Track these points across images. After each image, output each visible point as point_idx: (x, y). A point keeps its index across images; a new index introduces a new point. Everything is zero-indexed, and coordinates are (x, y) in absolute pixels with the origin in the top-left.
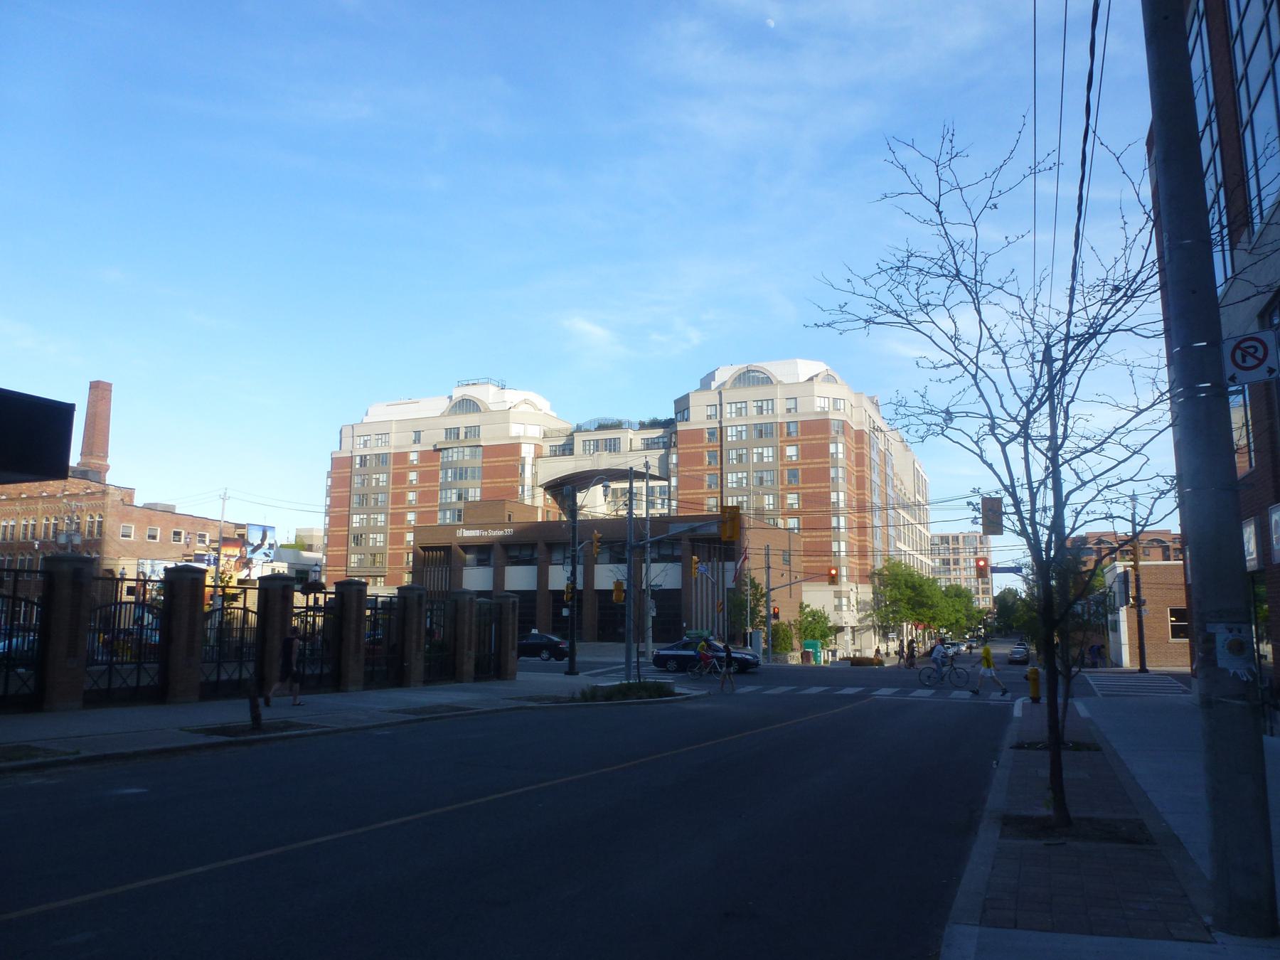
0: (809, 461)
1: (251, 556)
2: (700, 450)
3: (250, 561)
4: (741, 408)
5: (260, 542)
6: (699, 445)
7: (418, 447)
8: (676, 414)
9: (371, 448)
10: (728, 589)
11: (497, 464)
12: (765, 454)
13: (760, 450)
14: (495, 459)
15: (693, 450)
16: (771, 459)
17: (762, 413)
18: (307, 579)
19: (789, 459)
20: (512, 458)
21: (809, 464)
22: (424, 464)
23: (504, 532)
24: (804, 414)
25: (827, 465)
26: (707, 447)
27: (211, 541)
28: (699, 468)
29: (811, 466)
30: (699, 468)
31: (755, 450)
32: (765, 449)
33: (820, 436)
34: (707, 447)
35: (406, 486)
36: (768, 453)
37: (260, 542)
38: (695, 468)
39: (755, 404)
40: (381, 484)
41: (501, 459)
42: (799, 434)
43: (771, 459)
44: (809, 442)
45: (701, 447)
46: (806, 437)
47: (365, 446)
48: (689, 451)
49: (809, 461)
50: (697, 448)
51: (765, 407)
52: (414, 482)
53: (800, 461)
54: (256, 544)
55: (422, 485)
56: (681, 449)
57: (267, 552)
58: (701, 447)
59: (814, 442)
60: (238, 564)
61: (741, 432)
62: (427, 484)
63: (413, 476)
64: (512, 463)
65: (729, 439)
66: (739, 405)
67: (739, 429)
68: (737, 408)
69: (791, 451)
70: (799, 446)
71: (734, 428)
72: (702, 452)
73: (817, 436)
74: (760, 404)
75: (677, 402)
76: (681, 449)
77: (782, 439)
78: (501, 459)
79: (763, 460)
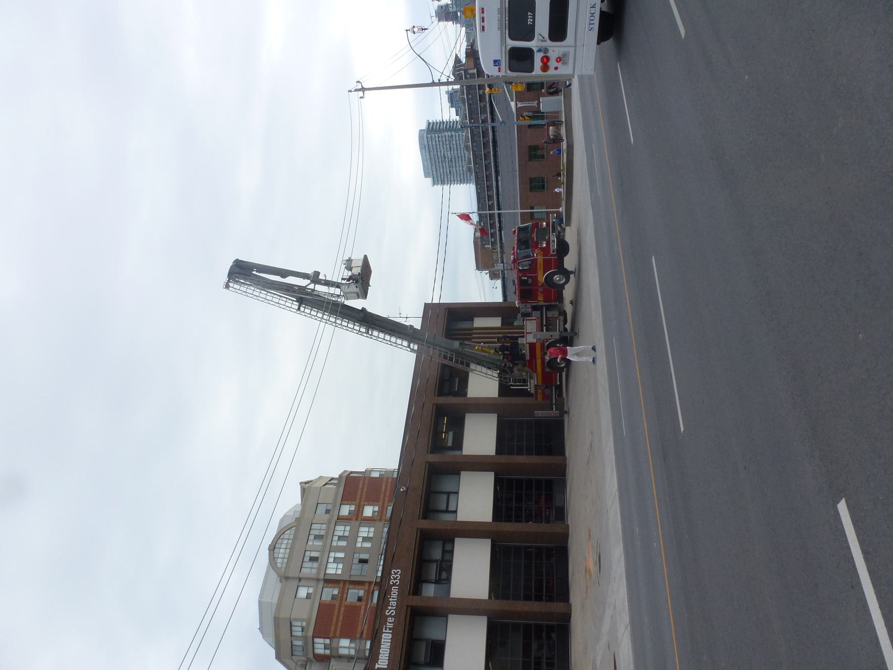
0: (382, 496)
2: (343, 609)
6: (336, 610)
12: (366, 535)
13: (360, 540)
15: (341, 618)
16: (372, 529)
17: (323, 536)
19: (376, 514)
21: (385, 494)
23: (394, 585)
24: (336, 498)
25: (390, 480)
26: (341, 600)
29: (388, 494)
31: (359, 545)
34: (341, 600)
36: (364, 532)
39: (310, 543)
42: (354, 502)
43: (372, 529)
44: (364, 494)
45: (339, 609)
46: (358, 497)
48: (340, 623)
49: (382, 496)
50: (339, 612)
51: (317, 533)
53: (381, 502)
56: (335, 632)
58: (339, 609)
59: (365, 491)
61: (335, 558)
65: (339, 572)
66: (307, 559)
67: (331, 560)
69: (368, 511)
70: (366, 503)
71: (329, 565)
72: (346, 606)
74: (312, 537)
75: (278, 657)
76: (335, 632)
77: (354, 519)
79: (371, 538)
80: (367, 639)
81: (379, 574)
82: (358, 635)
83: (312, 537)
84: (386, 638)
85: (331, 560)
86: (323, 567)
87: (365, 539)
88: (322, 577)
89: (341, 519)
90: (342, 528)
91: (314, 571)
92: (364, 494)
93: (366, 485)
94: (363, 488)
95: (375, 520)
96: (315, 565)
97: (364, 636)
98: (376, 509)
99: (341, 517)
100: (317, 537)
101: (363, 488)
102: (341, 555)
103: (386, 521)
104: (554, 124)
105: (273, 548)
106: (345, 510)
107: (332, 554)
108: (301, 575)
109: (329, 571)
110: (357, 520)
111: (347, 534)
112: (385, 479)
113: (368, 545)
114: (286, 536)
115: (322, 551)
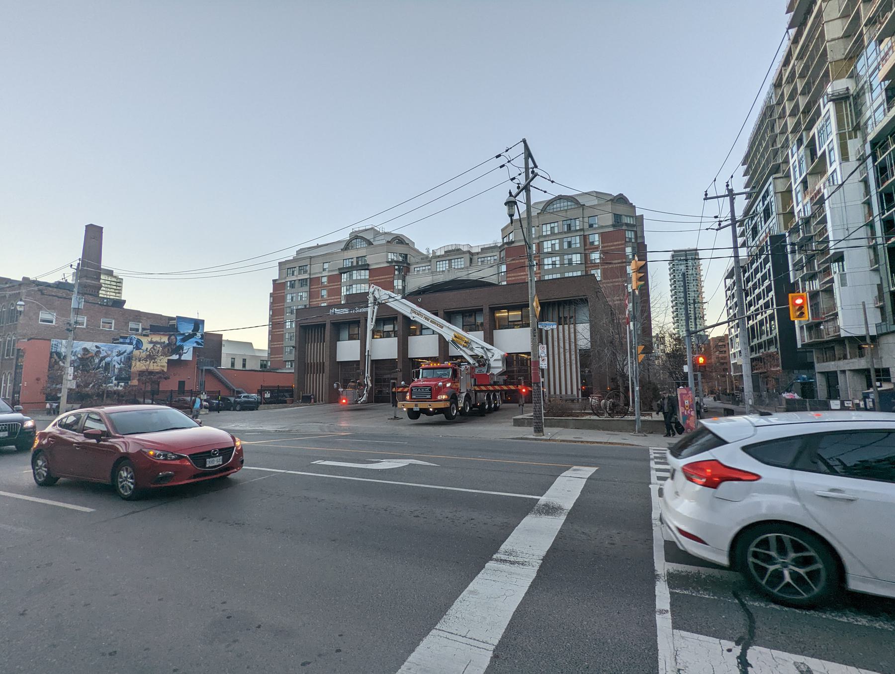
1: (182, 344)
3: (181, 348)
4: (554, 227)
5: (190, 331)
7: (326, 273)
8: (503, 239)
9: (297, 276)
10: (580, 350)
11: (378, 281)
13: (570, 257)
14: (377, 278)
18: (153, 348)
20: (389, 276)
22: (331, 284)
24: (602, 227)
27: (143, 329)
28: (522, 274)
30: (522, 274)
31: (566, 257)
32: (574, 256)
33: (617, 243)
35: (319, 299)
36: (577, 258)
37: (190, 331)
38: (519, 274)
40: (303, 299)
41: (381, 277)
46: (606, 245)
47: (293, 275)
52: (325, 297)
54: (187, 334)
55: (330, 298)
57: (200, 341)
60: (166, 349)
61: (555, 244)
62: (333, 298)
63: (324, 293)
64: (388, 279)
66: (552, 225)
67: (553, 242)
68: (551, 228)
69: (596, 256)
73: (615, 243)
74: (569, 222)
75: (502, 230)
77: (586, 248)
78: (381, 277)
80: (507, 281)
81: (546, 278)
82: (508, 275)
83: (569, 222)
84: (346, 311)
85: (553, 242)
86: (547, 239)
87: (570, 260)
88: (541, 240)
89: (585, 238)
90: (578, 241)
91: (544, 234)
92: (608, 248)
93: (617, 247)
94: (614, 245)
95: (586, 263)
96: (549, 233)
97: (508, 279)
98: (598, 261)
99: (587, 237)
100: (569, 226)
101: (614, 245)
102: (557, 248)
103: (586, 271)
104: (614, 405)
105: (560, 198)
106: (596, 239)
107: (557, 241)
108: (540, 226)
109: (545, 243)
110: (585, 250)
111: (573, 246)
112: (624, 260)
113: (566, 262)
114: (569, 203)
115: (559, 233)
